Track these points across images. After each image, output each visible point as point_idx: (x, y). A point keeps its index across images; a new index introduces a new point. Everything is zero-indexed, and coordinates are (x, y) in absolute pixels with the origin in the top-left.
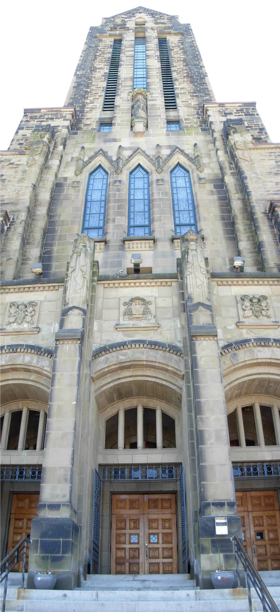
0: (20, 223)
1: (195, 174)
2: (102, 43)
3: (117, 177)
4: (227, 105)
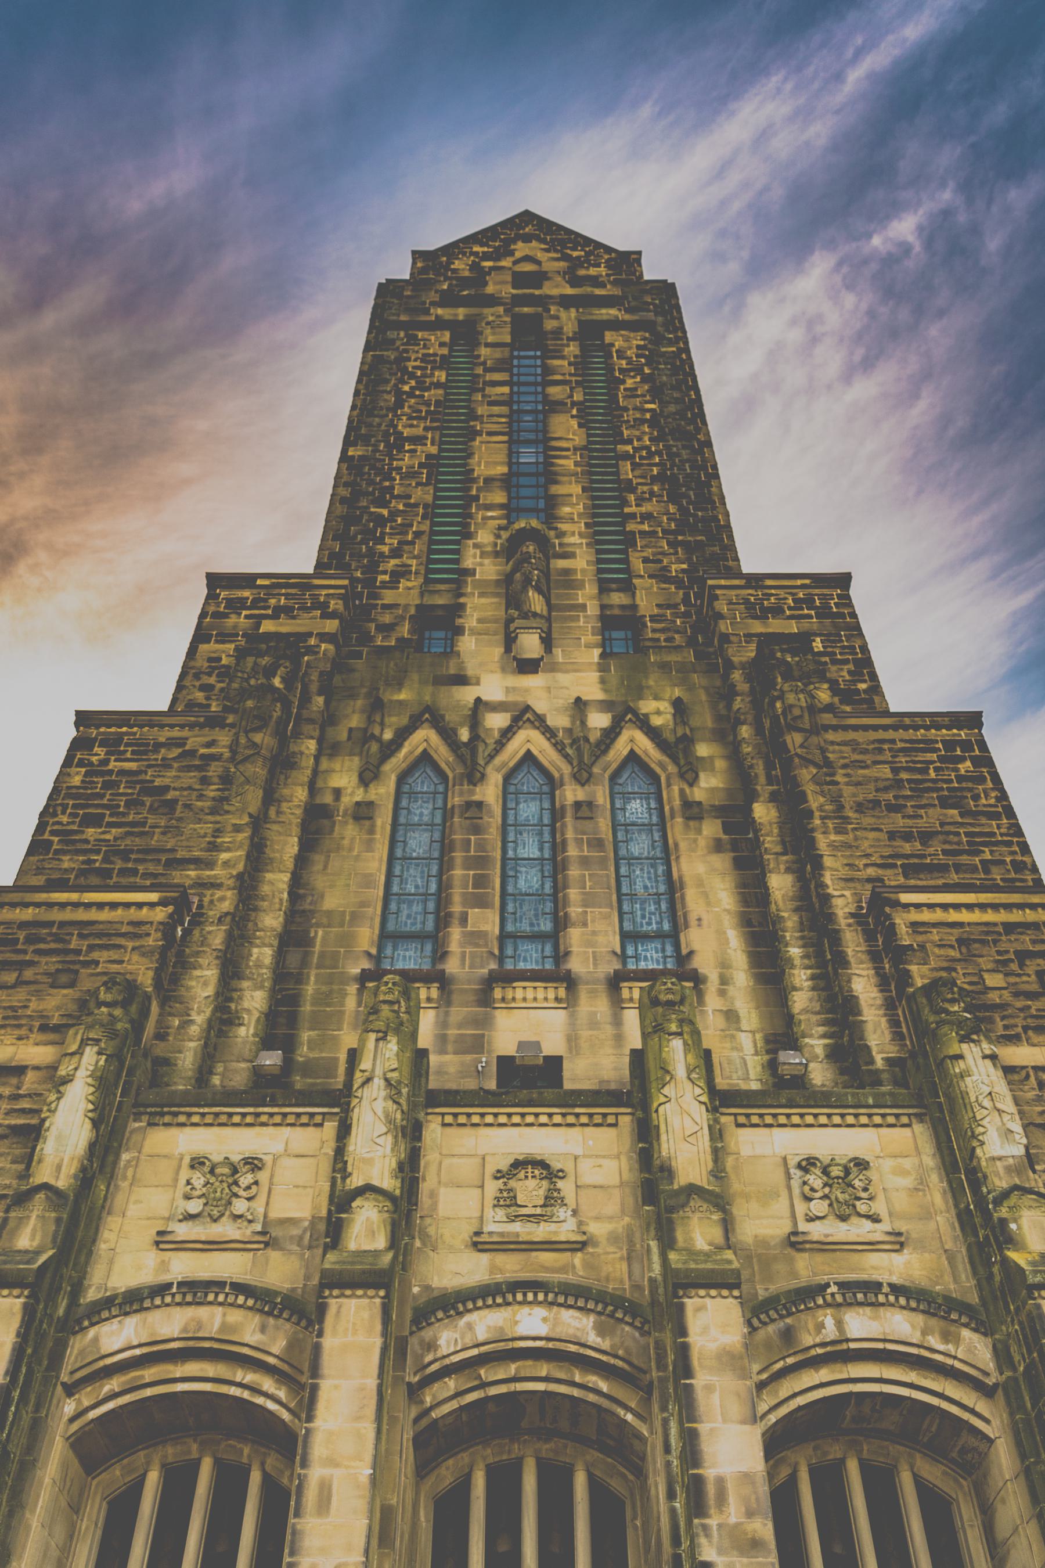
0: (220, 919)
1: (676, 789)
2: (416, 348)
3: (472, 793)
4: (769, 582)
